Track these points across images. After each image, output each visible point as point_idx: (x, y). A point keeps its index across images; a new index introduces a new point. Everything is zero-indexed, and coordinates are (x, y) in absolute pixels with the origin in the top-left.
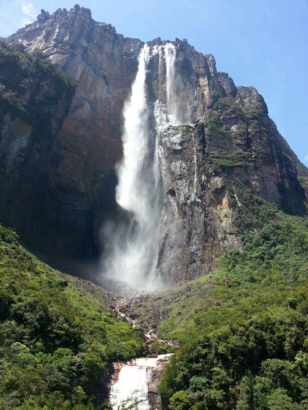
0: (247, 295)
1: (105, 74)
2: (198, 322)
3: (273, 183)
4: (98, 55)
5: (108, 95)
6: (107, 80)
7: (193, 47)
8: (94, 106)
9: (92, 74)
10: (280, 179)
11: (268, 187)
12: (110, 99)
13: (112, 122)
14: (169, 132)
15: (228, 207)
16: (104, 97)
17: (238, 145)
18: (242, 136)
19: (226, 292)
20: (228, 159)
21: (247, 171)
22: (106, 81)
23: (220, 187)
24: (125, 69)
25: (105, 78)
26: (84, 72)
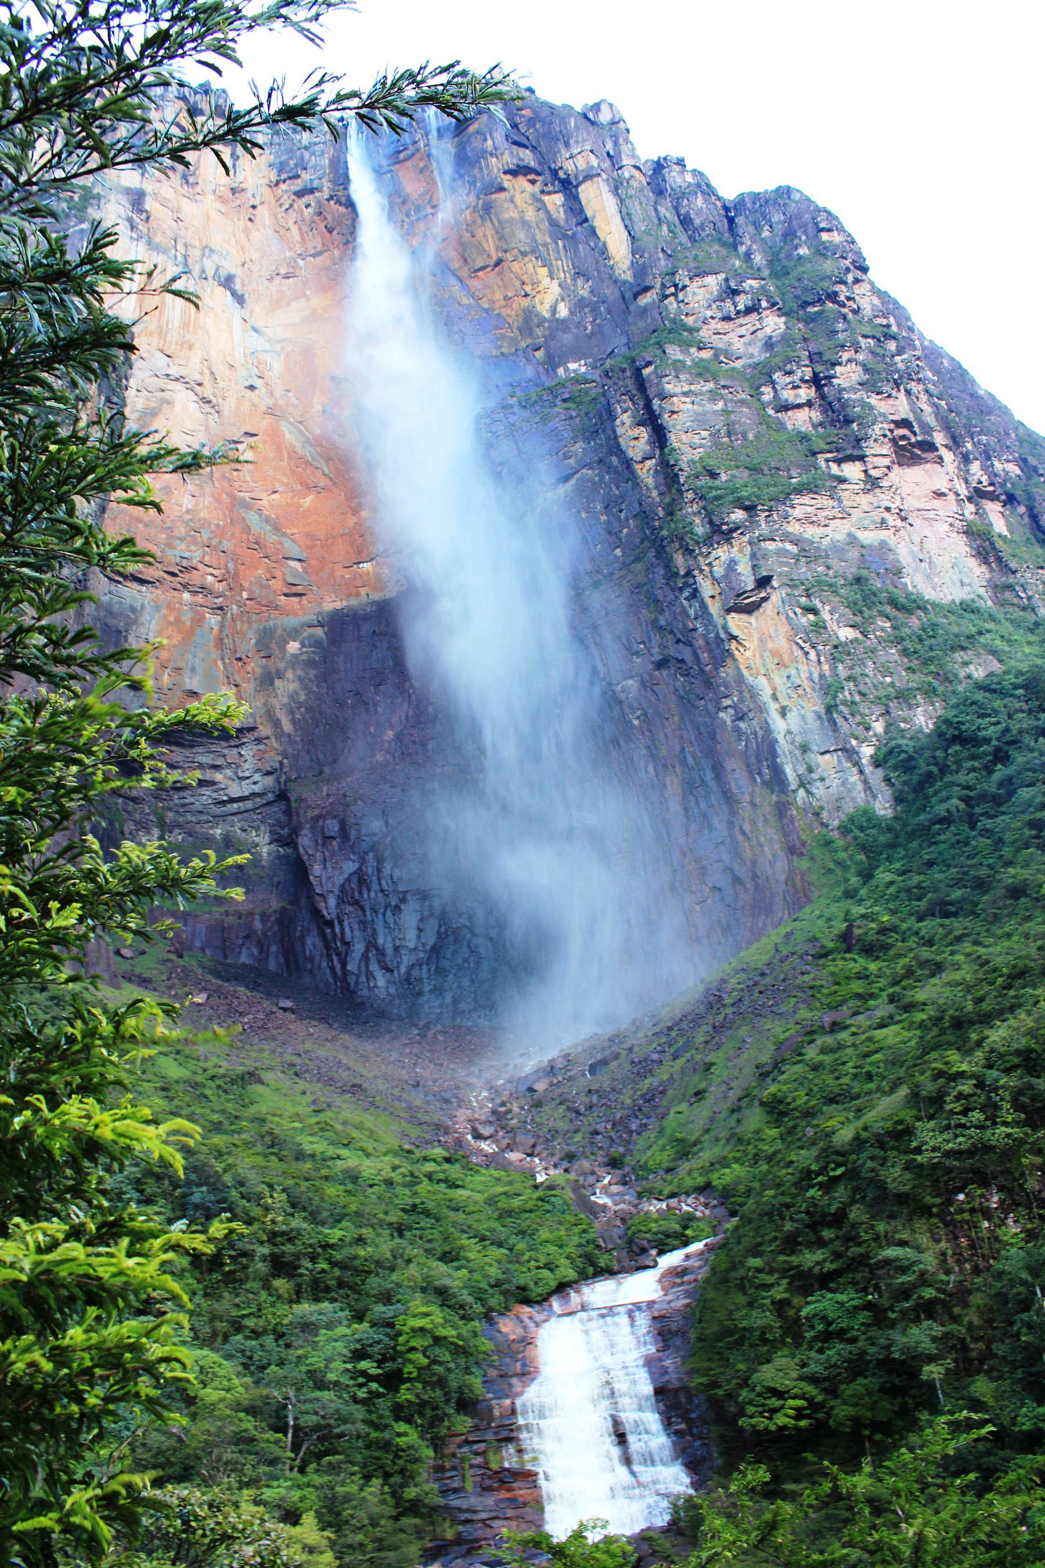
0: (937, 968)
1: (229, 267)
2: (777, 1110)
3: (946, 527)
4: (188, 208)
5: (254, 342)
6: (238, 287)
7: (530, 90)
8: (207, 391)
10: (970, 508)
11: (931, 545)
12: (262, 356)
13: (287, 436)
14: (512, 419)
15: (798, 653)
17: (786, 407)
18: (789, 373)
19: (859, 976)
20: (754, 469)
21: (839, 500)
22: (234, 293)
23: (751, 585)
24: (294, 229)
25: (227, 282)
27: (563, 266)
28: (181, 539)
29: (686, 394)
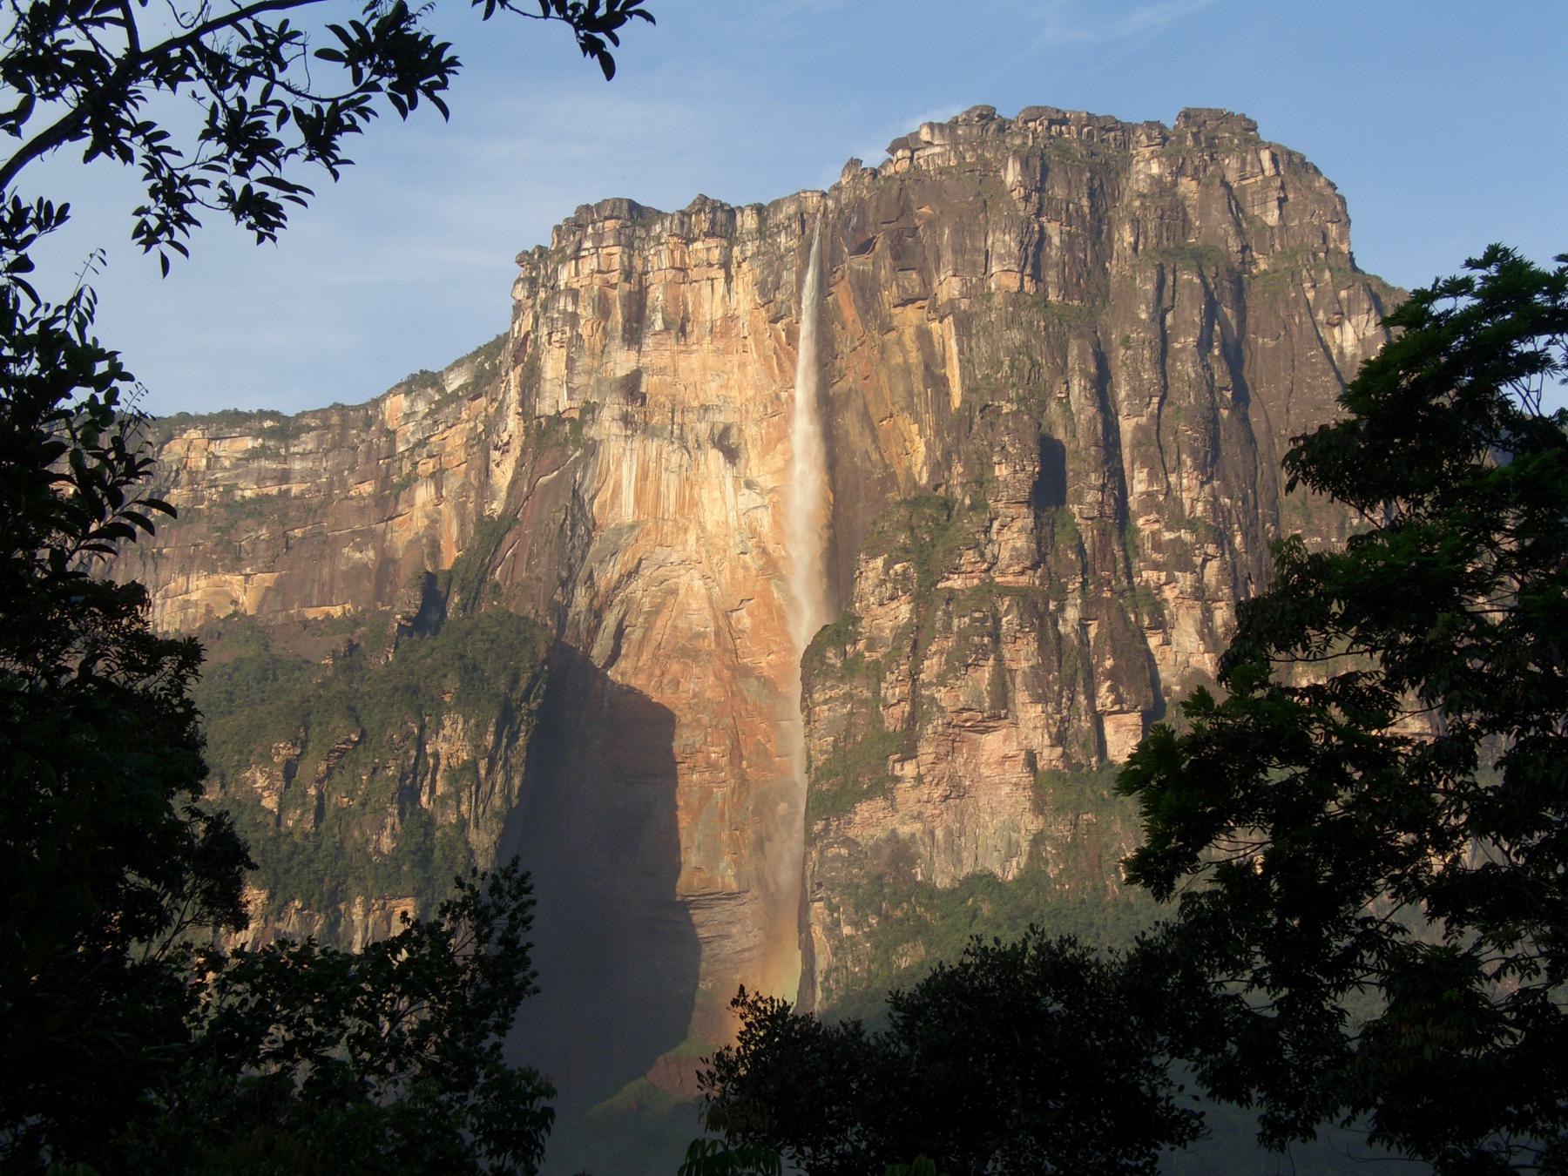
5: (748, 499)
9: (675, 459)
16: (733, 522)
26: (643, 475)
27: (929, 418)
28: (687, 726)
29: (826, 702)
